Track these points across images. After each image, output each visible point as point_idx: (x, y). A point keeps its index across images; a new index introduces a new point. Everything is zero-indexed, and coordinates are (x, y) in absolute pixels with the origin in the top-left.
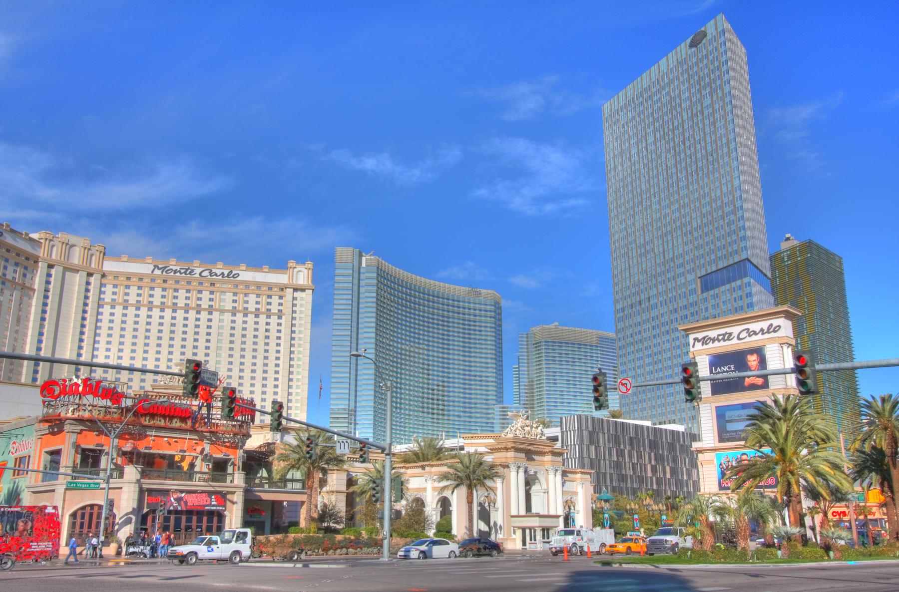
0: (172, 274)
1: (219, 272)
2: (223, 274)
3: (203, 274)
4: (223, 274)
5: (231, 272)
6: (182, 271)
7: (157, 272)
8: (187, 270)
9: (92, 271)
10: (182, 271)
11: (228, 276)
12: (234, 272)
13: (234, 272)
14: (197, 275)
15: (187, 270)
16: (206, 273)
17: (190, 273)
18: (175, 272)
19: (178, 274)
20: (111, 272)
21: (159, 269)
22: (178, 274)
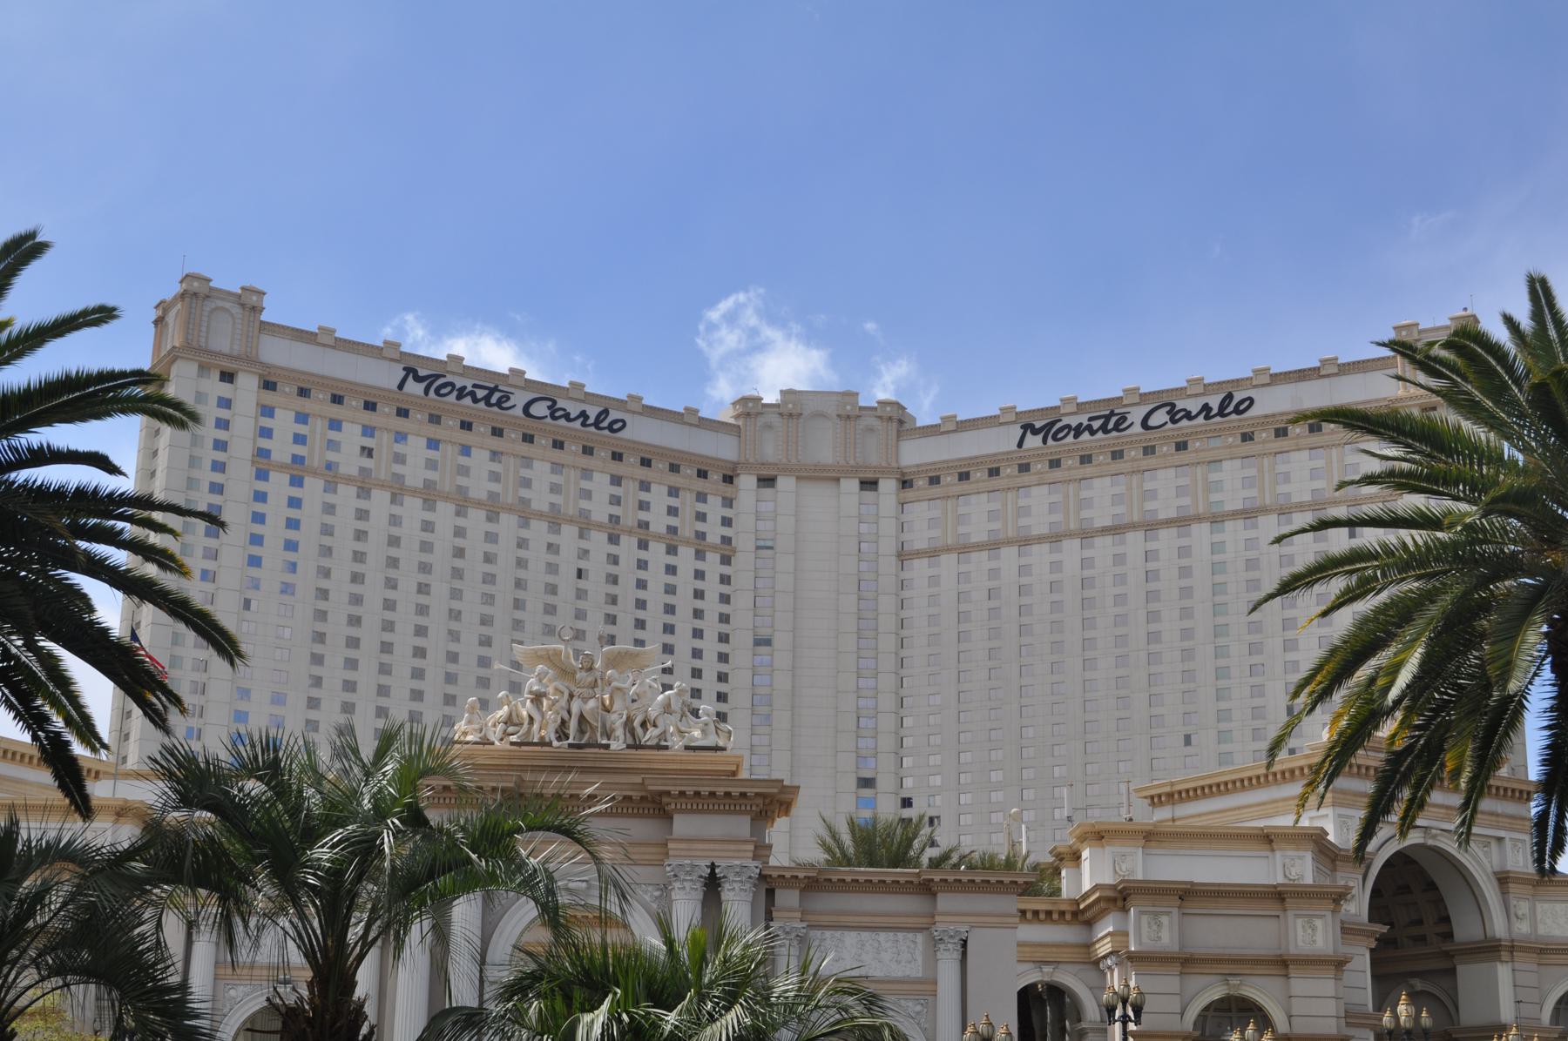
0: (1070, 439)
1: (1194, 406)
2: (1206, 408)
3: (1153, 422)
4: (1206, 408)
5: (1230, 396)
6: (1096, 424)
7: (1033, 441)
8: (1107, 418)
9: (870, 476)
10: (1096, 424)
11: (1221, 413)
12: (1238, 397)
13: (1238, 397)
14: (1137, 428)
15: (1107, 418)
16: (1160, 417)
17: (1116, 428)
18: (1078, 431)
19: (1086, 436)
20: (920, 469)
21: (1035, 432)
22: (1086, 436)
